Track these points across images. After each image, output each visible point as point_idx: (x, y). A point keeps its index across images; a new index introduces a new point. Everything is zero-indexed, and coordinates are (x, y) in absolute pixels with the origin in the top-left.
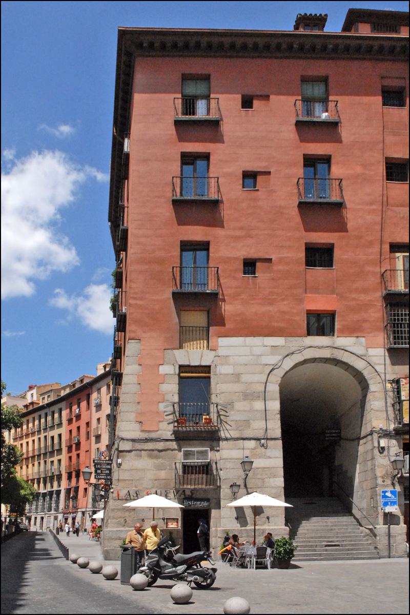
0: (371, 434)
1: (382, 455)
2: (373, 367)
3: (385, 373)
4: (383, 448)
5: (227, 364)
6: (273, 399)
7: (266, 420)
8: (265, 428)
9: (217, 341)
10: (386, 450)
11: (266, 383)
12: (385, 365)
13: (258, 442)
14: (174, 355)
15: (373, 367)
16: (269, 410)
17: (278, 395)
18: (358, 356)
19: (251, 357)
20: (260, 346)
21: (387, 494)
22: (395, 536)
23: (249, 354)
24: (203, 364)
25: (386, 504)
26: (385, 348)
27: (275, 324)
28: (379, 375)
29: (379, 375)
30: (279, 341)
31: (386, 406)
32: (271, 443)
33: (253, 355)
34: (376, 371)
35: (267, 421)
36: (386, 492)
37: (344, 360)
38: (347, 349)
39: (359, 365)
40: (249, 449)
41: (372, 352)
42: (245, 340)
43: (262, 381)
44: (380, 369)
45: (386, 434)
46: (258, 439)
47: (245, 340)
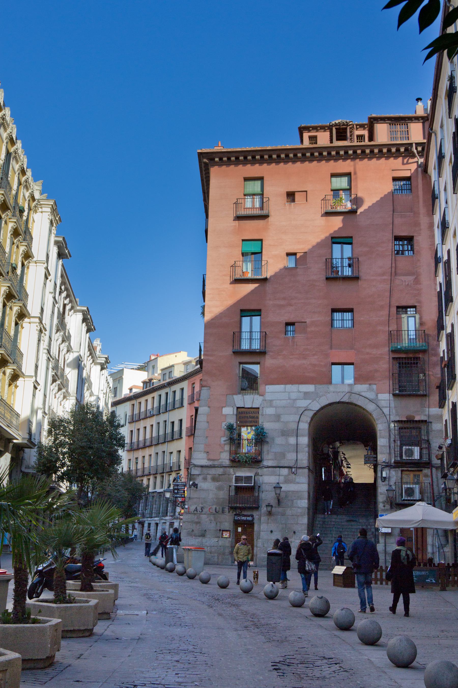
1: (383, 483)
4: (385, 478)
5: (271, 406)
6: (303, 436)
7: (297, 452)
10: (387, 479)
11: (299, 422)
12: (390, 407)
13: (290, 469)
17: (306, 432)
19: (289, 401)
27: (307, 374)
30: (310, 388)
32: (300, 471)
37: (359, 403)
39: (370, 407)
41: (381, 396)
42: (285, 388)
44: (386, 411)
45: (388, 466)
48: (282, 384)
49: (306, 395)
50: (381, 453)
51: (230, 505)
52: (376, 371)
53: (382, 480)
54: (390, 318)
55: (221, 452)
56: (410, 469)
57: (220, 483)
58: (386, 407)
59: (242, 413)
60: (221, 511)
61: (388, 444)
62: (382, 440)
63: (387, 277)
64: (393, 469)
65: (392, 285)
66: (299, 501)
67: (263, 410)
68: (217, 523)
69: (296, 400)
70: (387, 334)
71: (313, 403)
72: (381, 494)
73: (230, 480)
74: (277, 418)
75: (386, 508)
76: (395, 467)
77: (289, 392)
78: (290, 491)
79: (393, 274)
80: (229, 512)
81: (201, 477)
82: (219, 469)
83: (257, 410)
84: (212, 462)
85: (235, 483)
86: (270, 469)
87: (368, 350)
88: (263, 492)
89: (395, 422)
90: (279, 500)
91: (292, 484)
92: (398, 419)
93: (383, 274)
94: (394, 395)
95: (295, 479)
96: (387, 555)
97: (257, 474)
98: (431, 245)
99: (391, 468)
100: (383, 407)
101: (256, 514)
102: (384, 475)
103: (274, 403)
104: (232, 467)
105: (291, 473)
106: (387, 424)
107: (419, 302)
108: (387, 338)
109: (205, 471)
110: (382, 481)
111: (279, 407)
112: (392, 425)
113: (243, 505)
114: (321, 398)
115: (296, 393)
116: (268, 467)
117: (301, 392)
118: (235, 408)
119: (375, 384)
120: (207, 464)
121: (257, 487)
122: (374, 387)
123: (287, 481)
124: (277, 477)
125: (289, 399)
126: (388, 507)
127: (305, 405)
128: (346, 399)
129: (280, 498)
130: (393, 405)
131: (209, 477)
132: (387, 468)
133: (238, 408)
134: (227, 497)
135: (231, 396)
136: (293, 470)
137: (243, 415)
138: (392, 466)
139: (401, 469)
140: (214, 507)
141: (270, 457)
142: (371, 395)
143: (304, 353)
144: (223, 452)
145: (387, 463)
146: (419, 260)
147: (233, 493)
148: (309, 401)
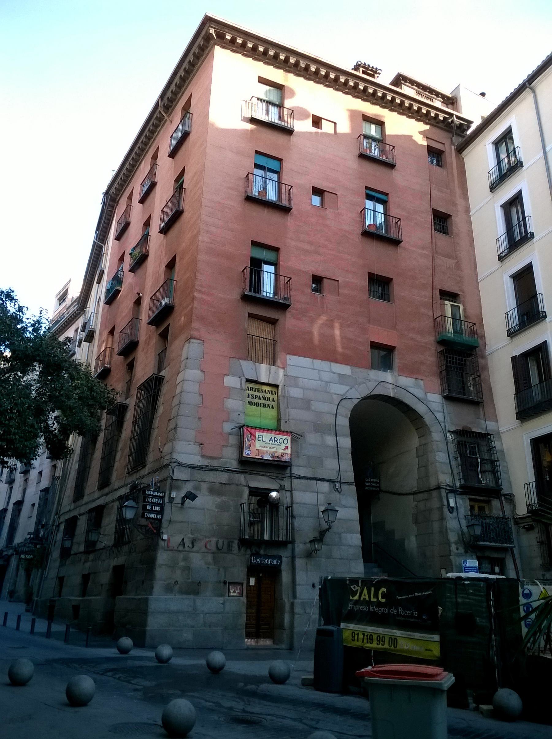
4: (452, 508)
5: (296, 386)
7: (339, 459)
10: (455, 510)
11: (336, 415)
13: (332, 485)
19: (320, 382)
20: (328, 372)
23: (318, 379)
30: (346, 370)
32: (345, 487)
34: (436, 418)
38: (409, 389)
39: (420, 408)
40: (322, 493)
44: (440, 416)
45: (452, 491)
50: (443, 473)
53: (449, 510)
54: (434, 302)
56: (478, 497)
58: (438, 411)
63: (428, 252)
64: (460, 496)
66: (349, 536)
68: (219, 570)
73: (240, 494)
74: (306, 404)
75: (459, 551)
76: (461, 494)
77: (319, 370)
79: (434, 251)
80: (239, 549)
82: (221, 473)
84: (208, 460)
86: (302, 481)
94: (446, 398)
95: (340, 501)
100: (435, 411)
101: (285, 554)
102: (452, 504)
103: (301, 382)
104: (241, 472)
106: (442, 434)
107: (462, 291)
109: (199, 475)
110: (451, 513)
112: (449, 436)
115: (328, 373)
116: (300, 478)
117: (334, 373)
119: (422, 380)
120: (200, 464)
122: (421, 383)
125: (320, 380)
126: (462, 550)
127: (342, 393)
133: (248, 381)
139: (468, 496)
140: (214, 540)
142: (420, 393)
148: (347, 388)
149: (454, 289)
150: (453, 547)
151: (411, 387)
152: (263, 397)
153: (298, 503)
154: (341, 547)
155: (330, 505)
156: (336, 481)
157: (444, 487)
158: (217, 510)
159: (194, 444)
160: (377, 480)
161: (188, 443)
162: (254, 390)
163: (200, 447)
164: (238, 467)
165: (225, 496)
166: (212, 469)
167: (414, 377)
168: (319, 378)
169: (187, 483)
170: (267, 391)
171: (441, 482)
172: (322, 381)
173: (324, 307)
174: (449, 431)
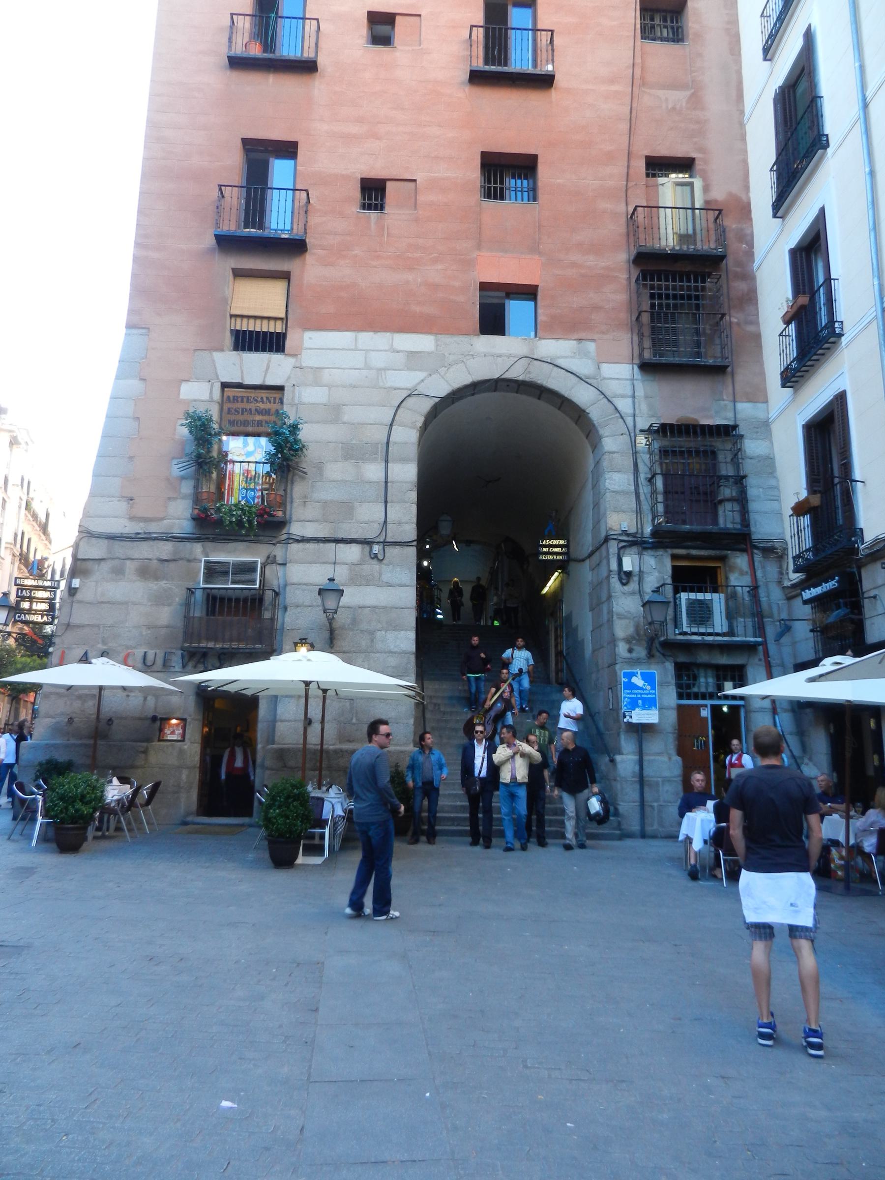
0: (607, 539)
1: (626, 588)
2: (609, 401)
3: (634, 416)
4: (629, 574)
5: (317, 383)
6: (404, 460)
7: (386, 502)
8: (383, 519)
9: (302, 338)
10: (636, 579)
11: (391, 425)
12: (634, 397)
13: (367, 548)
14: (213, 361)
15: (609, 401)
16: (392, 482)
17: (413, 451)
18: (581, 379)
19: (365, 372)
20: (385, 351)
21: (635, 680)
22: (657, 784)
23: (362, 366)
24: (270, 382)
25: (633, 705)
26: (633, 364)
27: (417, 309)
28: (622, 418)
29: (622, 418)
30: (423, 342)
31: (637, 485)
32: (392, 551)
33: (371, 369)
34: (616, 409)
35: (389, 505)
36: (635, 674)
38: (560, 362)
39: (582, 396)
41: (608, 370)
43: (385, 423)
44: (625, 406)
45: (634, 542)
46: (366, 542)
47: (356, 336)
48: (348, 330)
49: (413, 358)
50: (617, 510)
51: (187, 645)
52: (597, 308)
53: (620, 579)
54: (630, 184)
55: (169, 498)
56: (694, 552)
57: (163, 584)
58: (623, 396)
59: (235, 399)
60: (159, 662)
61: (632, 488)
62: (616, 476)
63: (623, 87)
64: (650, 552)
65: (634, 105)
66: (391, 635)
67: (293, 392)
69: (385, 369)
70: (623, 220)
71: (430, 378)
72: (621, 617)
75: (634, 655)
77: (367, 351)
78: (364, 607)
79: (637, 82)
81: (105, 567)
82: (162, 543)
83: (276, 395)
85: (206, 581)
86: (308, 545)
87: (575, 257)
88: (285, 609)
89: (648, 431)
90: (332, 631)
91: (372, 587)
92: (656, 422)
93: (612, 81)
94: (647, 367)
95: (380, 574)
96: (646, 789)
97: (270, 560)
98: (729, 23)
99: (645, 549)
100: (616, 396)
103: (326, 376)
104: (198, 539)
105: (368, 558)
106: (626, 438)
107: (702, 150)
108: (623, 229)
109: (121, 549)
111: (337, 386)
113: (226, 645)
114: (451, 370)
117: (398, 352)
118: (218, 386)
121: (269, 595)
122: (591, 347)
123: (357, 580)
124: (330, 568)
125: (368, 367)
126: (641, 652)
128: (517, 373)
129: (336, 625)
130: (640, 392)
131: (130, 566)
132: (635, 549)
133: (225, 386)
134: (180, 623)
135: (206, 354)
136: (376, 548)
137: (239, 405)
138: (645, 542)
139: (670, 551)
141: (311, 511)
142: (584, 367)
143: (409, 255)
144: (175, 499)
145: (634, 535)
146: (700, 55)
147: (198, 612)
148: (421, 375)
149: (680, 150)
150: (622, 649)
151: (566, 357)
152: (256, 410)
153: (293, 584)
154: (373, 655)
155: (331, 582)
156: (378, 540)
157: (615, 537)
158: (150, 604)
159: (119, 501)
160: (562, 542)
161: (108, 499)
162: (239, 400)
163: (129, 503)
164: (194, 531)
165: (167, 580)
166: (147, 538)
167: (576, 337)
168: (366, 363)
169: (103, 563)
170: (265, 399)
171: (611, 529)
172: (371, 369)
173: (383, 235)
174: (641, 431)
